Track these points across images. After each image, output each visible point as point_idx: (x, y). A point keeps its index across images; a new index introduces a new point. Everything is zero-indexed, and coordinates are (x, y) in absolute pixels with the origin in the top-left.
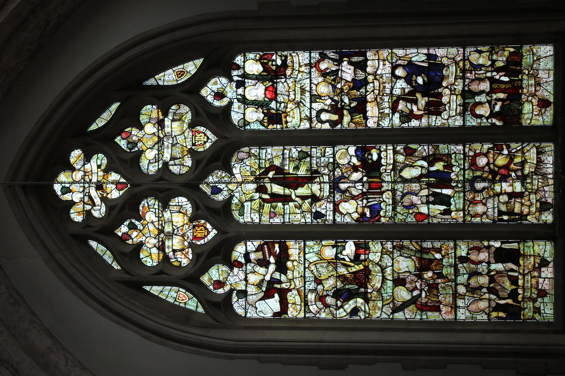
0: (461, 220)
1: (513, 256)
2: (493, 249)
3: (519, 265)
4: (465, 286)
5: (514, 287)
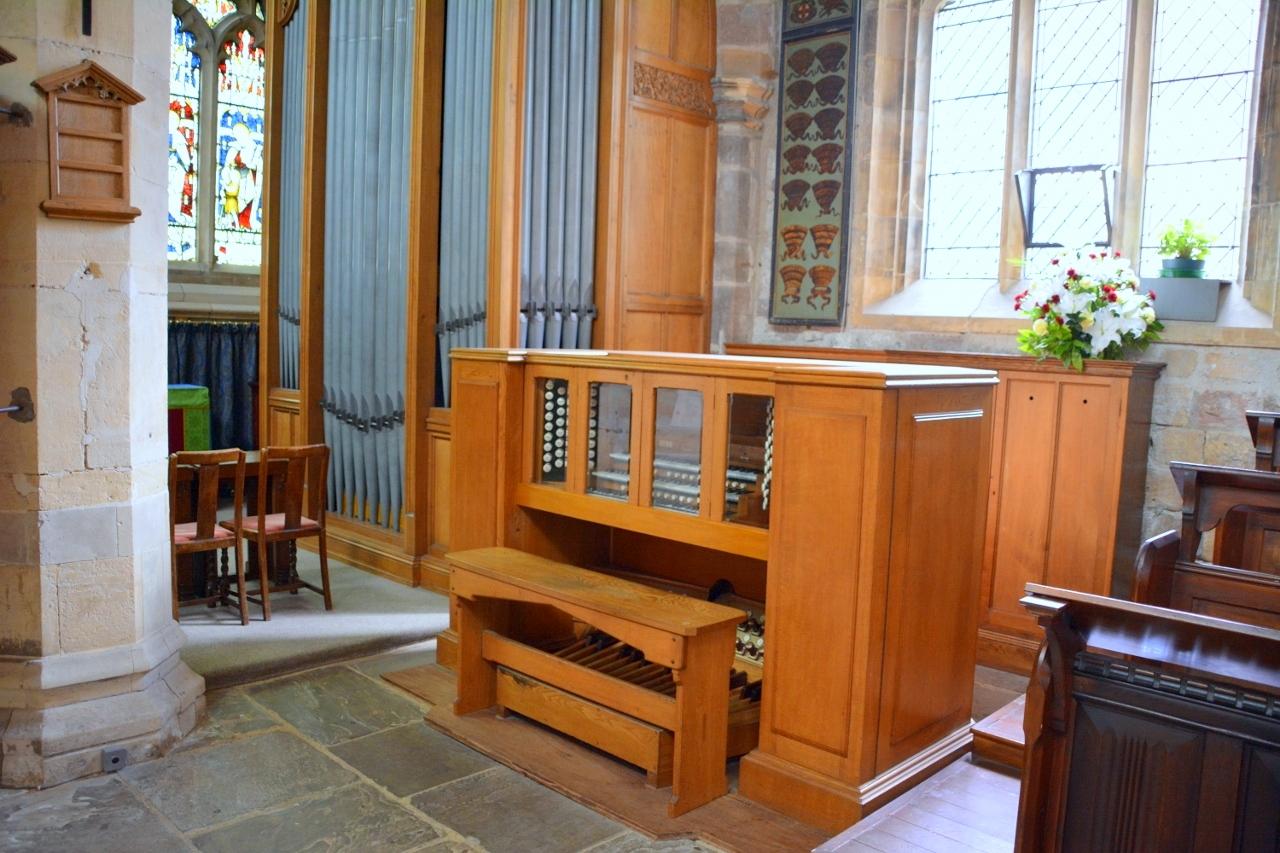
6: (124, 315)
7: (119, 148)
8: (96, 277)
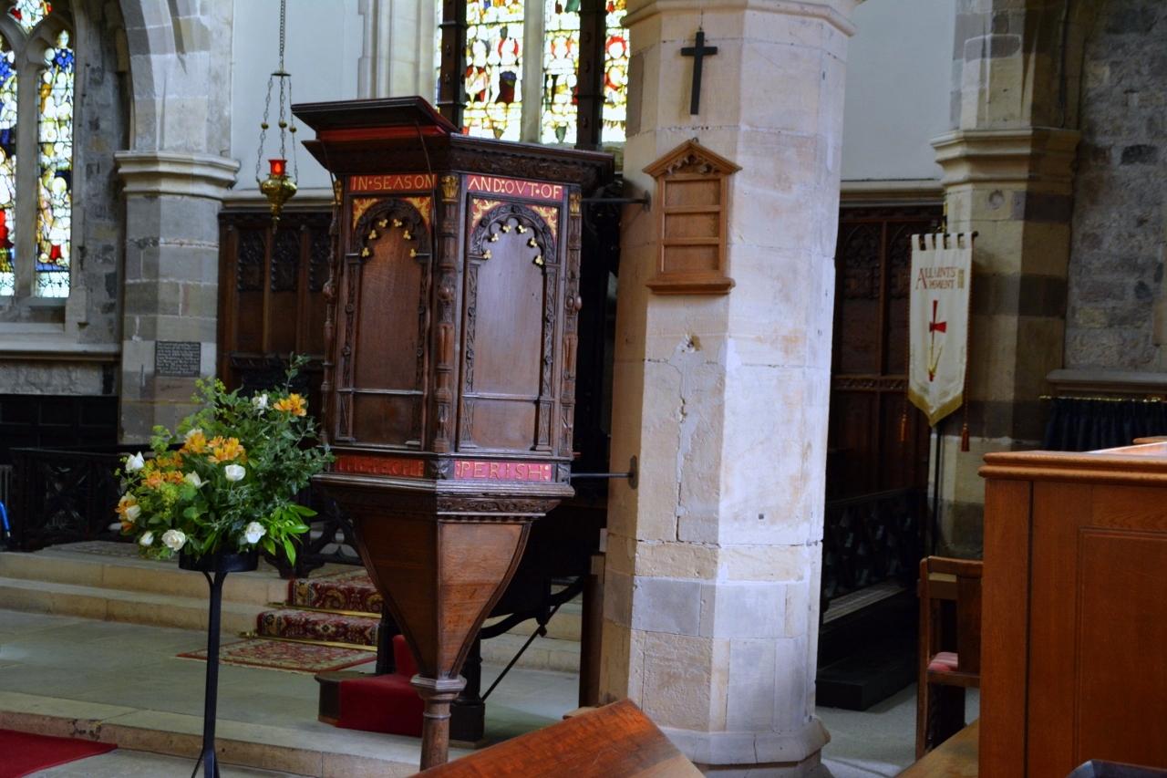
0: (548, 27)
1: (506, 95)
2: (514, 69)
3: (497, 102)
4: (475, 37)
5: (472, 97)
6: (719, 389)
7: (718, 219)
8: (697, 350)
